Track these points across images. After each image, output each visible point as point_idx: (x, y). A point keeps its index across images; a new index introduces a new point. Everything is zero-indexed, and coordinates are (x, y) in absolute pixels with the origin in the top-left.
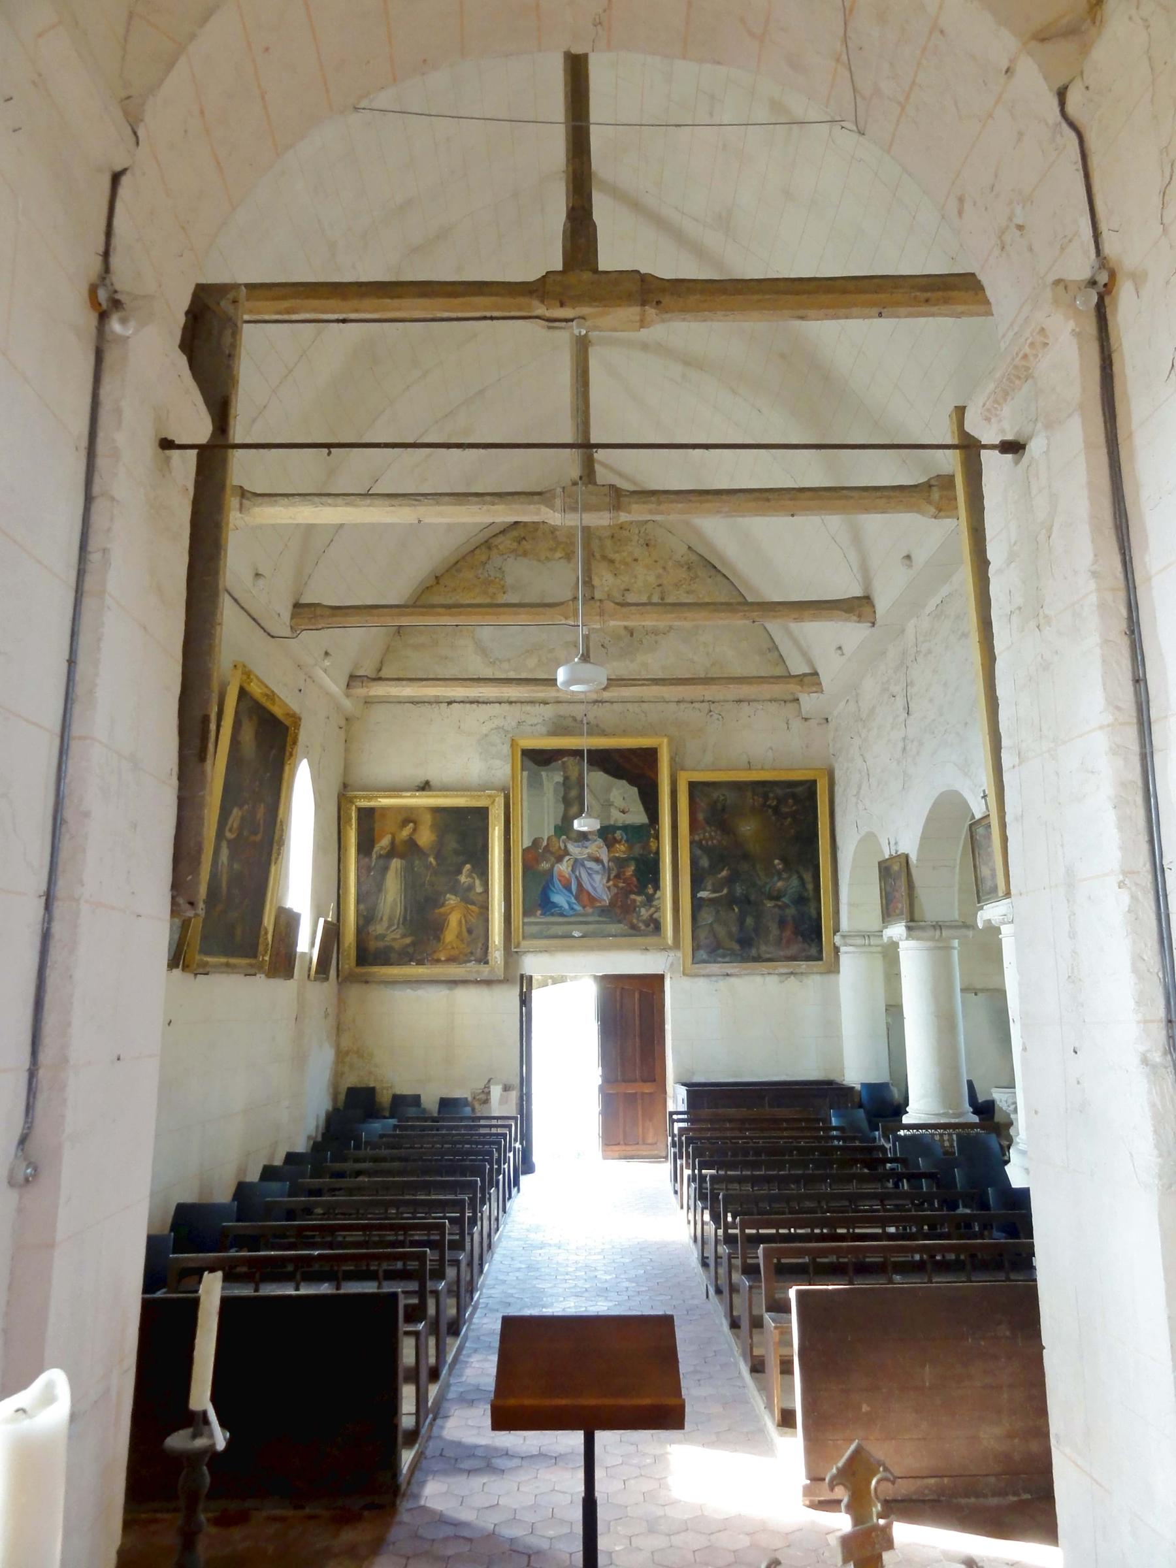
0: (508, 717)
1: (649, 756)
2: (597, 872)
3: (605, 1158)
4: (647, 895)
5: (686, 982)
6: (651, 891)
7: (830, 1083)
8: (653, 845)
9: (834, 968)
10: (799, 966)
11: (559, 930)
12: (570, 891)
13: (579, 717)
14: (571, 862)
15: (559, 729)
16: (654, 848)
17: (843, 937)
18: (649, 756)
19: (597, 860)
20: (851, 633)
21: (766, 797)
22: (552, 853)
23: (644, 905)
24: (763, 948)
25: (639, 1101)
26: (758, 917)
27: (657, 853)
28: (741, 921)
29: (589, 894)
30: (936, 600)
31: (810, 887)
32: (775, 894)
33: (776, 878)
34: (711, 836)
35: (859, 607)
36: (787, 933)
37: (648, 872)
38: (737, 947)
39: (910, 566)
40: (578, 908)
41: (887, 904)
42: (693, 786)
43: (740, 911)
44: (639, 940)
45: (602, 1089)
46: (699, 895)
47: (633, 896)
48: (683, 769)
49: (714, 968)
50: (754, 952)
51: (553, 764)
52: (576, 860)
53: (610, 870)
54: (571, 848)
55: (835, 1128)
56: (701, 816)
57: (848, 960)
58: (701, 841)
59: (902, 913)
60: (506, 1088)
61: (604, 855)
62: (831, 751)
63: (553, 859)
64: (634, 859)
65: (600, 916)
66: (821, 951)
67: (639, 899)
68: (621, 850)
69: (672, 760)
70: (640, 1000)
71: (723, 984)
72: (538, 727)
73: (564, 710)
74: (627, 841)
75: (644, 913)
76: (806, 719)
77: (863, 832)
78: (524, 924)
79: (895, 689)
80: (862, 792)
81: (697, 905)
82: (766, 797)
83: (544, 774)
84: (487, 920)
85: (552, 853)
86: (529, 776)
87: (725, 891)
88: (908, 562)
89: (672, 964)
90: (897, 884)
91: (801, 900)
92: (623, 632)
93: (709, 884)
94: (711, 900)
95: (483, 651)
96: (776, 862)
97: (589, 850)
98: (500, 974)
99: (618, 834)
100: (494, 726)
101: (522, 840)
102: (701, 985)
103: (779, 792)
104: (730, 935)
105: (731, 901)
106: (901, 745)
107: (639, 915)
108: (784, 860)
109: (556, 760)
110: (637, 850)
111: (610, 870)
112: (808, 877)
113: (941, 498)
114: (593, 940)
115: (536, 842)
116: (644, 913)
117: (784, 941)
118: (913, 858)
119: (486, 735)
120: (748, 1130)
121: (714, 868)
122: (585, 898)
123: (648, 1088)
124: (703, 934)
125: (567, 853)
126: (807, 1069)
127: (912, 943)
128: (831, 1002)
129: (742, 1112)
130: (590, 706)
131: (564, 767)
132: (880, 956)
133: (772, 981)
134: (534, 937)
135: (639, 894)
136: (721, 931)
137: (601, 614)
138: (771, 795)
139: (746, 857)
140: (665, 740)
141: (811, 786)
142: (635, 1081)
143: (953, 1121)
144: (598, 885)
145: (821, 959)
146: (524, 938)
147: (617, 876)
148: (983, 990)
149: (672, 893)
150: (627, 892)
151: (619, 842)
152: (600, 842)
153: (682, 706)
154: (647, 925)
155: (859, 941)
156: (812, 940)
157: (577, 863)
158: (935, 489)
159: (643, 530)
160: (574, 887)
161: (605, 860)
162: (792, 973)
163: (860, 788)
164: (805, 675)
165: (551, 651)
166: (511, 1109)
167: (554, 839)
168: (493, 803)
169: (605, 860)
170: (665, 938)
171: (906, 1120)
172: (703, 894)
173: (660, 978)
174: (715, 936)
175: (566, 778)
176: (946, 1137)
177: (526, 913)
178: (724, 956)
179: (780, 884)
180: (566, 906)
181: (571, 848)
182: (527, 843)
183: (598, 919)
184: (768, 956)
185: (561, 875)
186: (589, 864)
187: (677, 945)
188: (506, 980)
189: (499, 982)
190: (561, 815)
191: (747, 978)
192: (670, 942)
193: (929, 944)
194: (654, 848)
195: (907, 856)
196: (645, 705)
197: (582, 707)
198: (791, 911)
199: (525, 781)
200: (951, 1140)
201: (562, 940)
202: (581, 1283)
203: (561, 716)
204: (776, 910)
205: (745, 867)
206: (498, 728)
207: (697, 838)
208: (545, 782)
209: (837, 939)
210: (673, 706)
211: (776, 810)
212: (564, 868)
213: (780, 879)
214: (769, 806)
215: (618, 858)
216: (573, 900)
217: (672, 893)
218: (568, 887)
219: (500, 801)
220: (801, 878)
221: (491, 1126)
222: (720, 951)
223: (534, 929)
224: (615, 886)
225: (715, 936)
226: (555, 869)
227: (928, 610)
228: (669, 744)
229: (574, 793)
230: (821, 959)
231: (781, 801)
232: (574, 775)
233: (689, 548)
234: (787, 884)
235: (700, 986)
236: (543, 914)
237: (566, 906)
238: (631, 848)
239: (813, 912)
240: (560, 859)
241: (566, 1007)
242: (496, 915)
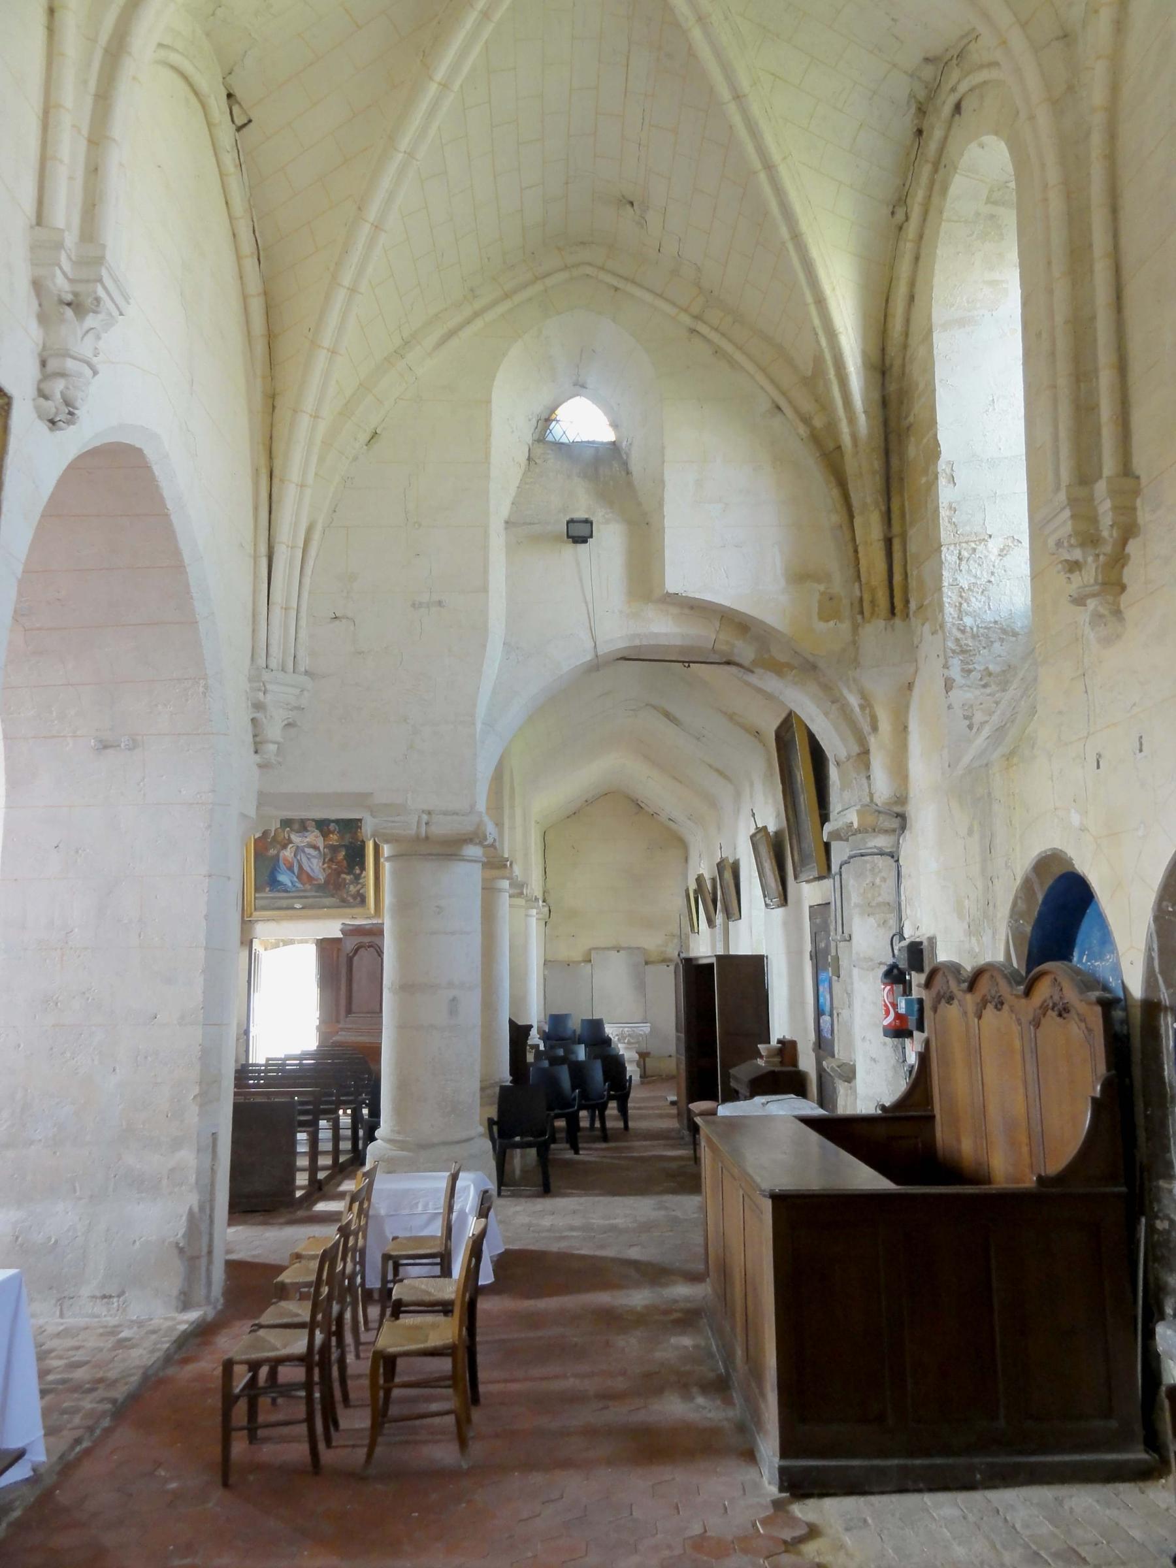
4: (354, 875)
6: (358, 872)
11: (284, 903)
12: (293, 872)
19: (316, 848)
23: (352, 883)
40: (299, 885)
44: (348, 910)
45: (318, 1028)
47: (343, 876)
54: (293, 837)
61: (320, 843)
64: (344, 846)
67: (348, 878)
68: (334, 839)
75: (353, 889)
99: (332, 826)
110: (347, 841)
114: (311, 909)
115: (265, 833)
116: (353, 889)
122: (304, 877)
125: (290, 841)
134: (264, 908)
135: (348, 874)
144: (316, 867)
147: (331, 860)
148: (624, 949)
150: (339, 873)
151: (333, 833)
152: (317, 833)
154: (354, 898)
157: (298, 850)
160: (296, 869)
177: (257, 890)
181: (293, 837)
183: (314, 894)
185: (285, 859)
192: (372, 911)
201: (285, 910)
212: (288, 853)
218: (291, 869)
238: (342, 838)
240: (285, 847)
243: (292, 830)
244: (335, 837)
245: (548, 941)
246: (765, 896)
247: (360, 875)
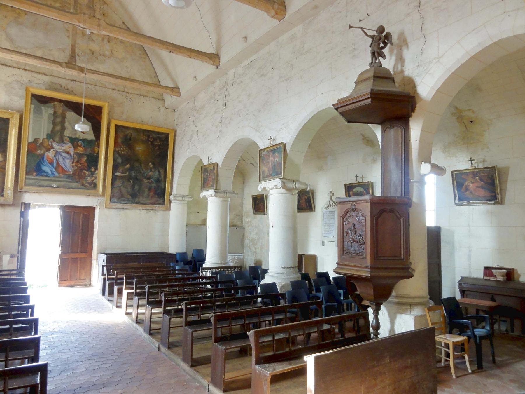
0: (26, 77)
1: (98, 110)
2: (67, 158)
3: (59, 286)
4: (91, 172)
5: (106, 211)
6: (93, 170)
7: (163, 253)
8: (96, 150)
9: (168, 209)
11: (46, 183)
12: (53, 165)
13: (63, 85)
14: (54, 152)
15: (52, 87)
16: (96, 151)
17: (175, 196)
18: (98, 110)
19: (68, 153)
20: (206, 69)
21: (149, 137)
22: (44, 147)
23: (89, 176)
25: (79, 261)
26: (140, 186)
27: (98, 153)
28: (133, 187)
29: (62, 168)
30: (249, 61)
31: (162, 176)
32: (148, 177)
34: (124, 150)
35: (214, 58)
36: (152, 194)
37: (93, 161)
38: (130, 197)
39: (246, 42)
40: (56, 174)
41: (204, 183)
42: (117, 127)
43: (133, 182)
45: (60, 256)
47: (85, 171)
48: (113, 118)
49: (119, 205)
50: (137, 200)
51: (49, 105)
52: (57, 151)
53: (74, 158)
54: (55, 145)
55: (177, 270)
56: (120, 140)
57: (175, 206)
59: (212, 186)
60: (12, 256)
62: (175, 123)
63: (44, 149)
65: (67, 178)
66: (164, 201)
67: (87, 173)
68: (80, 150)
69: (109, 114)
70: (83, 218)
71: (122, 212)
72: (41, 85)
73: (55, 80)
74: (84, 146)
75: (89, 179)
76: (166, 108)
77: (190, 156)
78: (26, 178)
79: (217, 97)
80: (193, 138)
81: (114, 179)
82: (149, 137)
83: (43, 108)
84: (4, 175)
85: (44, 147)
86: (35, 108)
87: (127, 174)
88: (245, 39)
89: (100, 203)
90: (207, 175)
91: (158, 181)
92: (88, 51)
94: (121, 176)
95: (11, 40)
96: (150, 164)
97: (64, 148)
98: (11, 201)
99: (80, 143)
100: (14, 79)
101: (28, 138)
102: (113, 212)
103: (155, 136)
104: (128, 193)
105: (129, 178)
106: (219, 120)
107: (87, 180)
108: (153, 164)
109: (50, 103)
110: (89, 151)
111: (74, 158)
112: (162, 172)
113: (278, 8)
114: (62, 189)
115: (36, 140)
116: (89, 179)
117: (150, 197)
118: (220, 165)
119: (10, 83)
120: (141, 272)
121: (123, 163)
122: (60, 169)
123: (83, 256)
124: (116, 191)
125: (52, 147)
126: (154, 247)
127: (215, 198)
128: (166, 222)
129: (135, 265)
130: (69, 81)
131: (54, 107)
132: (186, 205)
133: (143, 212)
134: (31, 185)
136: (124, 190)
137: (99, 25)
138: (151, 136)
139: (138, 160)
140: (107, 104)
141: (167, 135)
142: (78, 253)
143: (224, 266)
144: (68, 164)
145: (163, 204)
146: (25, 185)
147: (78, 162)
149: (103, 172)
150: (81, 170)
151: (80, 146)
152: (70, 145)
153: (115, 92)
155: (180, 199)
156: (161, 197)
157: (57, 153)
158: (276, 4)
159: (102, 7)
160: (55, 164)
161: (72, 154)
163: (192, 137)
164: (174, 88)
165: (50, 50)
166: (14, 267)
167: (46, 140)
168: (13, 117)
169: (72, 154)
170: (98, 191)
171: (204, 266)
172: (117, 174)
173: (93, 208)
174: (121, 192)
175: (55, 112)
176: (230, 272)
177: (27, 173)
178: (124, 200)
179: (151, 173)
180: (50, 172)
181: (56, 146)
182: (31, 140)
185: (48, 158)
186: (63, 154)
187: (103, 194)
188: (13, 205)
189: (9, 205)
190: (51, 129)
191: (133, 210)
192: (100, 193)
193: (221, 199)
194: (97, 151)
195: (217, 164)
196: (97, 88)
197: (65, 81)
198: (154, 185)
199: (32, 110)
200: (231, 272)
201: (48, 188)
202: (86, 351)
203: (53, 83)
204: (148, 184)
205: (137, 164)
206: (17, 81)
207: (117, 149)
208: (44, 112)
209: (171, 197)
210: (110, 91)
211: (152, 143)
212: (50, 154)
213: (151, 171)
214: (149, 141)
215: (78, 153)
216: (54, 170)
217: (103, 172)
218: (51, 163)
219: (17, 117)
221: (11, 275)
222: (123, 199)
223: (32, 181)
224: (76, 166)
225: (121, 192)
226: (46, 154)
227: (242, 65)
228: (109, 106)
229: (58, 120)
230: (163, 204)
231: (155, 139)
232: (60, 111)
233: (123, 23)
234: (154, 174)
235: (112, 213)
236: (37, 175)
237: (50, 172)
238: (85, 150)
239: (163, 186)
240: (48, 150)
241: (45, 220)
242: (10, 172)
243: (54, 141)
244: (81, 149)
245: (189, 213)
246: (455, 199)
247: (94, 172)
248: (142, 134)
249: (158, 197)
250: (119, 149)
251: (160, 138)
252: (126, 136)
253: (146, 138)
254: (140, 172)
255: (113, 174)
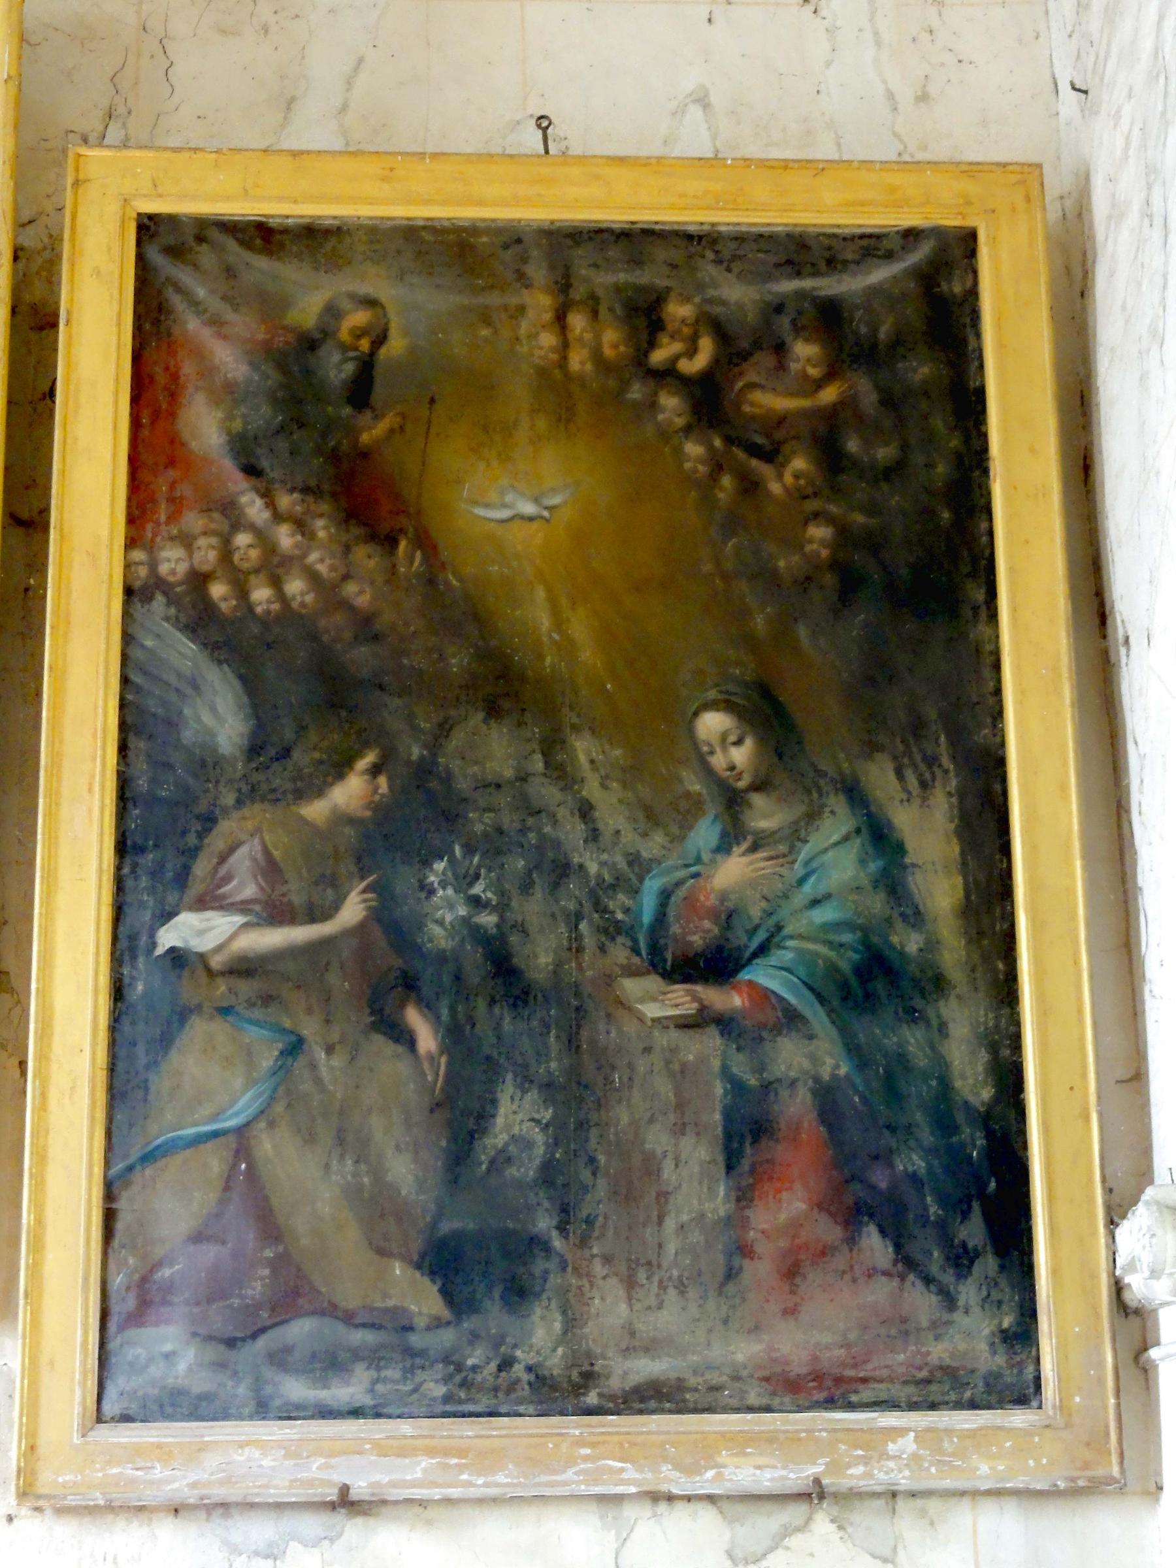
10: (873, 1444)
21: (645, 315)
24: (609, 1308)
26: (578, 1099)
28: (460, 1117)
31: (941, 891)
32: (699, 936)
33: (705, 833)
34: (293, 556)
38: (423, 1299)
42: (160, 240)
43: (455, 1036)
46: (168, 938)
49: (255, 1453)
50: (540, 1337)
58: (199, 580)
66: (1022, 1335)
82: (645, 315)
87: (353, 910)
91: (873, 980)
93: (243, 846)
94: (245, 968)
96: (712, 723)
103: (738, 294)
104: (376, 1208)
105: (389, 981)
108: (767, 712)
112: (929, 833)
117: (760, 1270)
124: (174, 1207)
136: (285, 1159)
138: (678, 311)
139: (504, 686)
145: (1025, 1394)
156: (962, 1260)
162: (814, 1494)
172: (195, 930)
174: (270, 1227)
179: (733, 872)
184: (646, 1368)
198: (809, 1057)
204: (707, 1047)
205: (494, 750)
207: (173, 562)
211: (709, 399)
214: (667, 375)
220: (880, 837)
222: (300, 1331)
230: (1025, 1394)
231: (742, 345)
234: (792, 878)
239: (973, 1085)
248: (540, 302)
249: (907, 1262)
250: (207, 555)
251: (829, 317)
252: (294, 358)
253: (612, 339)
254: (562, 870)
255: (125, 944)
